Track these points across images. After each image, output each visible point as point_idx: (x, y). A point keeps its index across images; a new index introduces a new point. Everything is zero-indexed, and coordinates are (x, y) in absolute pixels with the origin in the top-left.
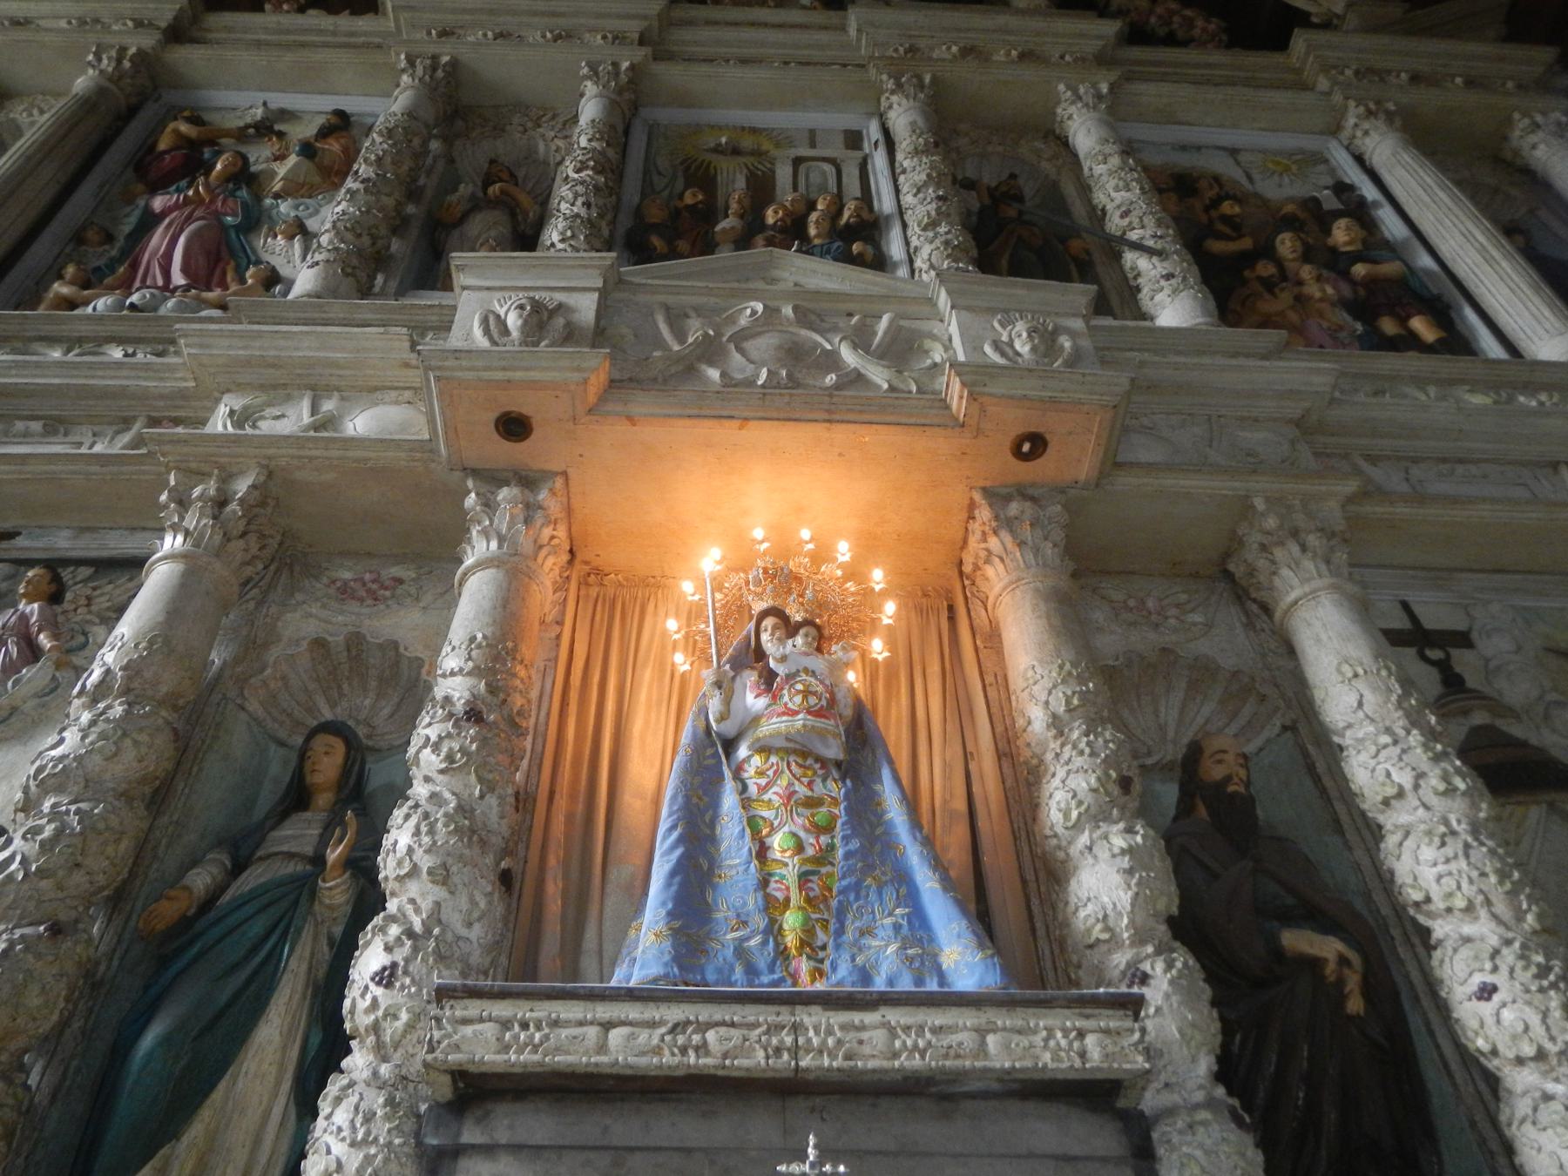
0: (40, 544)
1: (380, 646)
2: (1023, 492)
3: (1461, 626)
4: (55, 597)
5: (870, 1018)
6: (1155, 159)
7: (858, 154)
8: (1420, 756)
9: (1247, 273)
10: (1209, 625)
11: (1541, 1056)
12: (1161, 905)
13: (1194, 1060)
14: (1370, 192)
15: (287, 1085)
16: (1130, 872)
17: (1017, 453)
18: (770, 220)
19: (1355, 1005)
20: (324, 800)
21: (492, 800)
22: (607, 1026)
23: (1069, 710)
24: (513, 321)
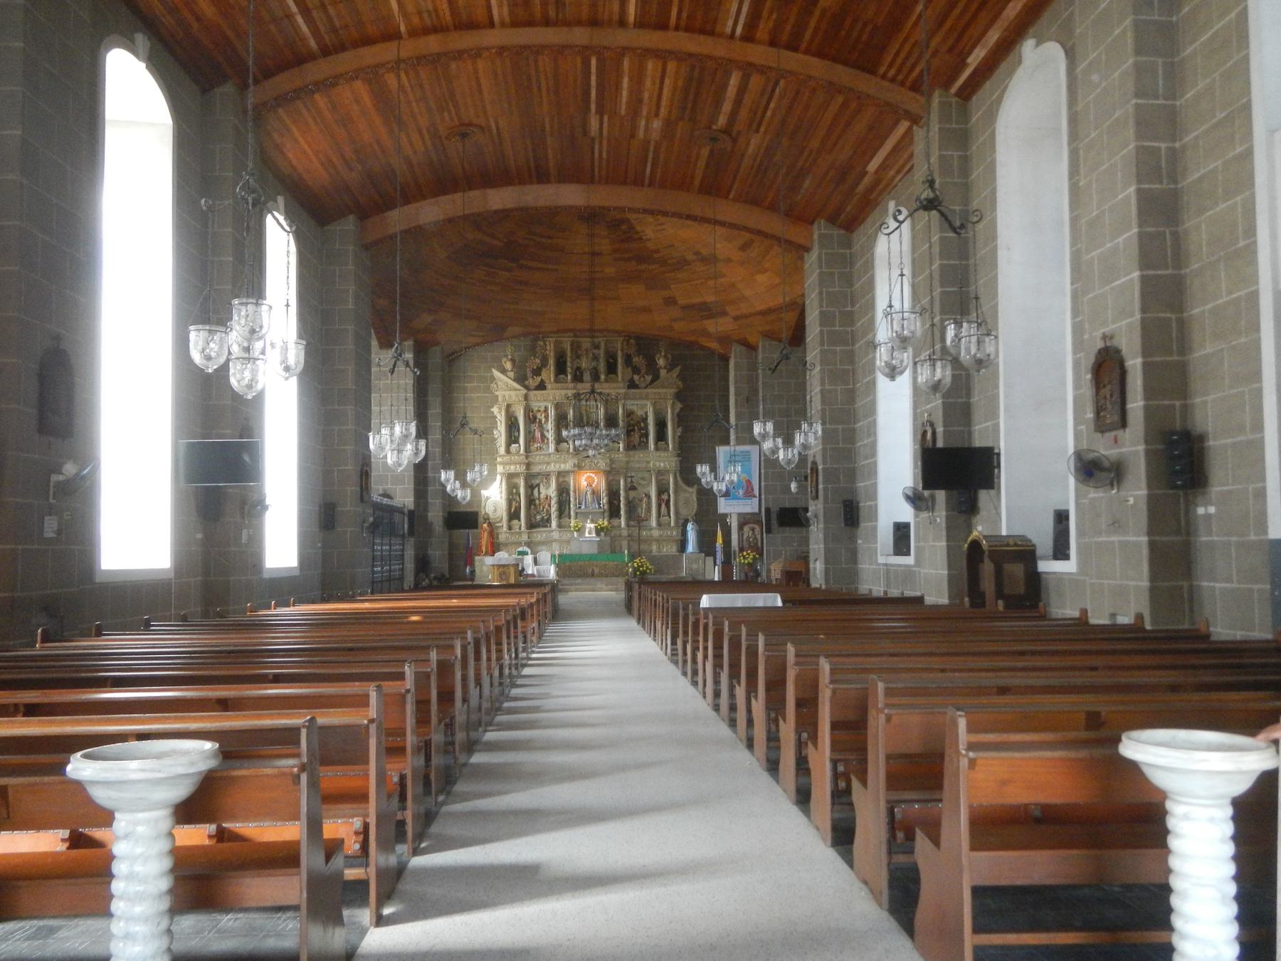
6: (628, 407)
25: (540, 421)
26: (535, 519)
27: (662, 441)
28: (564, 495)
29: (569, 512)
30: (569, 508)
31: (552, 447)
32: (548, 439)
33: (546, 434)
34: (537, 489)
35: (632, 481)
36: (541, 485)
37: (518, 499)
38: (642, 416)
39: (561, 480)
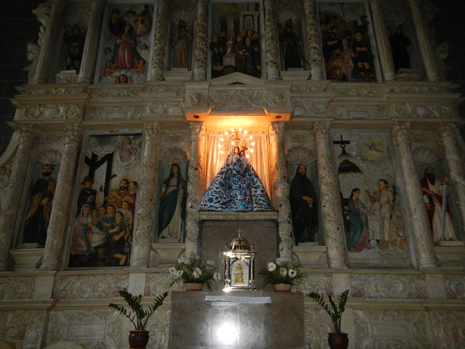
0: (124, 131)
1: (179, 149)
2: (278, 122)
3: (349, 140)
4: (130, 143)
5: (247, 213)
6: (323, 9)
7: (257, 13)
8: (326, 172)
9: (334, 52)
10: (307, 141)
11: (328, 214)
12: (286, 196)
13: (285, 216)
14: (369, 19)
15: (180, 216)
16: (282, 191)
17: (276, 118)
18: (238, 41)
19: (311, 205)
20: (176, 175)
21: (200, 181)
22: (218, 215)
23: (279, 165)
24: (195, 99)
25: (132, 31)
26: (88, 242)
27: (407, 65)
28: (174, 181)
29: (184, 225)
30: (184, 215)
31: (152, 71)
32: (145, 62)
33: (143, 54)
34: (104, 166)
35: (344, 153)
36: (117, 157)
37: (50, 188)
38: (355, 23)
39: (167, 145)
